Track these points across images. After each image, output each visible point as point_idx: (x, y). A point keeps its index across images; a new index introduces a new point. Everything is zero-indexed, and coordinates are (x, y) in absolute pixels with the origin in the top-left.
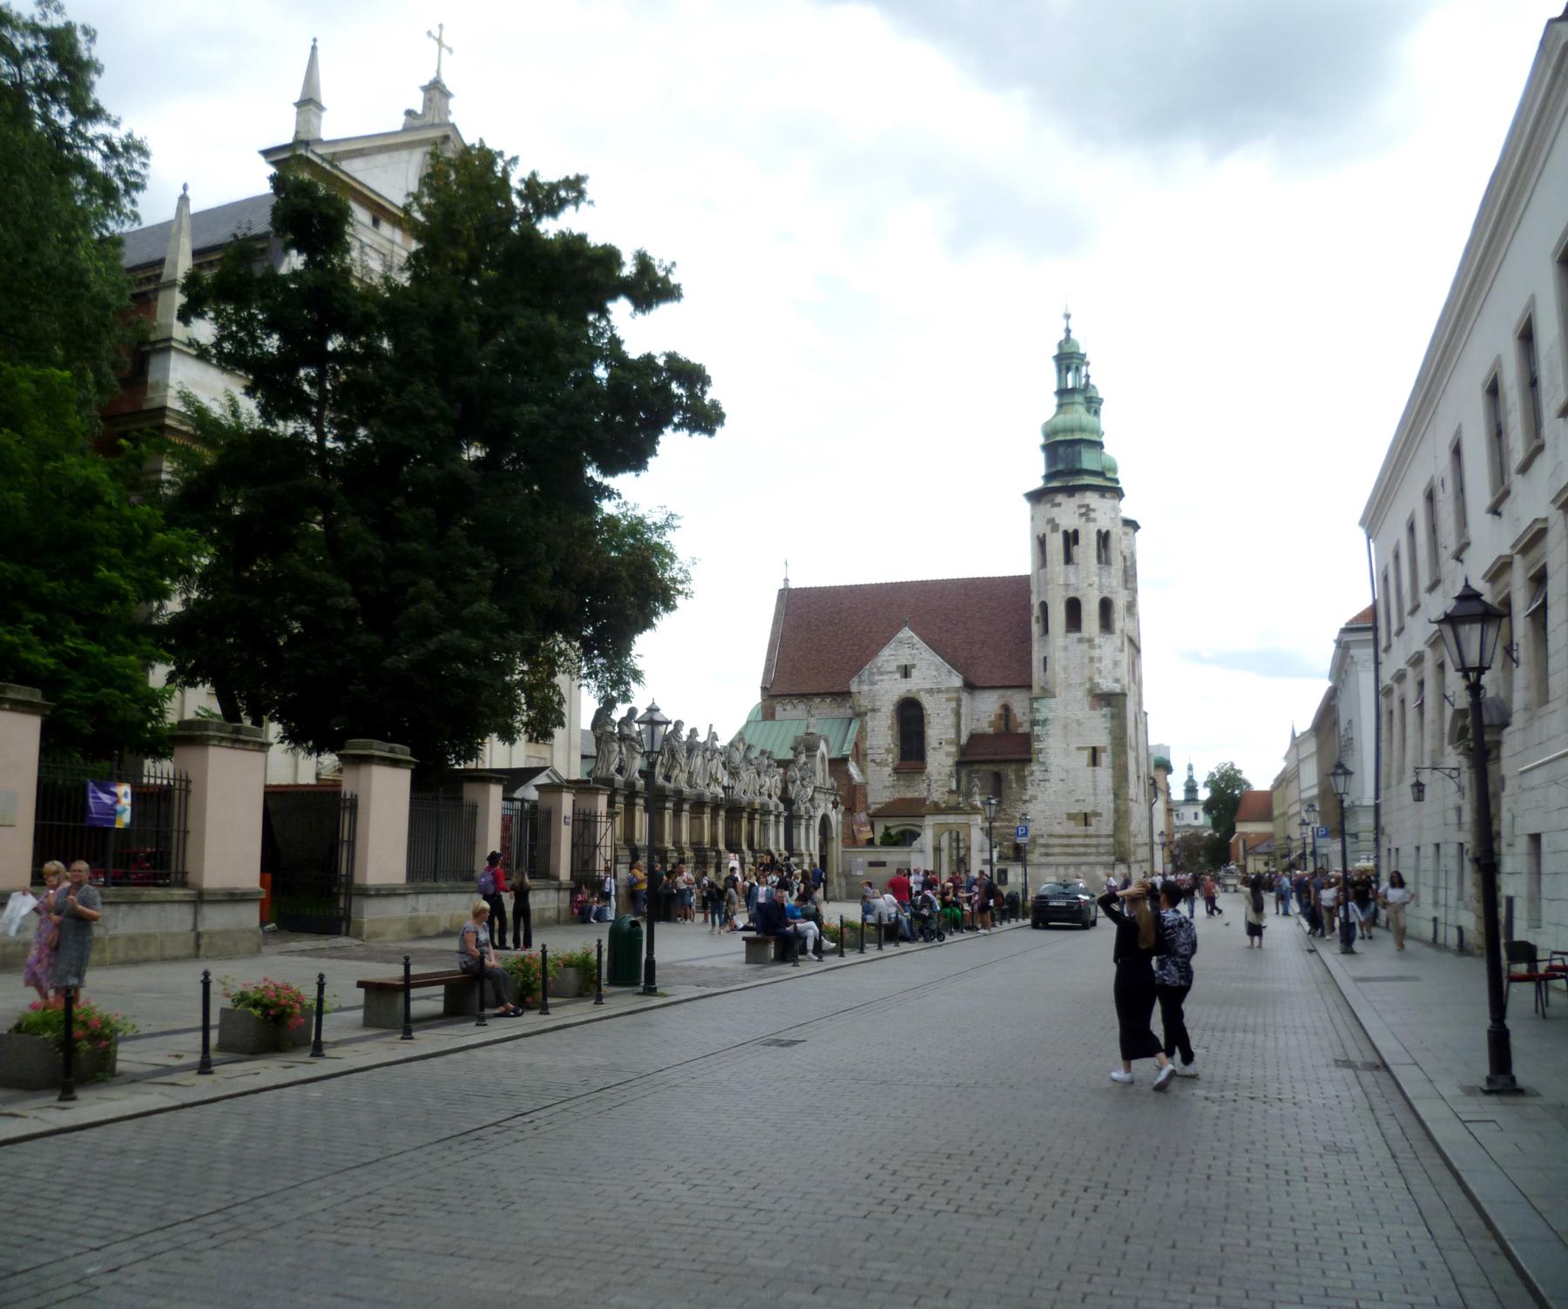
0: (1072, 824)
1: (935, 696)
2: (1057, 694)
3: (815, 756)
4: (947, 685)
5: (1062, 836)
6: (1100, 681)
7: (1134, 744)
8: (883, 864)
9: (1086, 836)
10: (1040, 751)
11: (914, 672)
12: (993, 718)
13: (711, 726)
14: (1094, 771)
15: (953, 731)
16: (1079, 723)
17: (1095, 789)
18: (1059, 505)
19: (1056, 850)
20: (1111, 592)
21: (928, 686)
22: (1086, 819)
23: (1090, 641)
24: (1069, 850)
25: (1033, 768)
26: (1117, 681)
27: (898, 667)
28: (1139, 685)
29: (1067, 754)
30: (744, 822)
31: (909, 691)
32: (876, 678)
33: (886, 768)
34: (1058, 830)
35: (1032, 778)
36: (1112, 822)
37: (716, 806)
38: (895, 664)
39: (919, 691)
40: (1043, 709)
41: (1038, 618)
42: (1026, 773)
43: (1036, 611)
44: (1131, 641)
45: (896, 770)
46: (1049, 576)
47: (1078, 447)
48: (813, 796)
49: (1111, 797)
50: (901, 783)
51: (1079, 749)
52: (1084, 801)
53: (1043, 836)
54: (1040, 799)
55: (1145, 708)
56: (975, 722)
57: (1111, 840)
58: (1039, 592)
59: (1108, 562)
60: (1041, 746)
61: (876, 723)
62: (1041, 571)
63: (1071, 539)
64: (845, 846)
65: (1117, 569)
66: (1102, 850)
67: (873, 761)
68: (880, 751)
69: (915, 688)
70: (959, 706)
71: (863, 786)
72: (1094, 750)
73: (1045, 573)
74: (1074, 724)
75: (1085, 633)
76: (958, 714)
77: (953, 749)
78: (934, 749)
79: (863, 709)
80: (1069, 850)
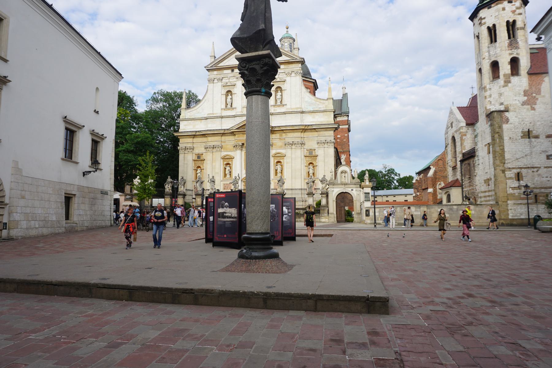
0: (485, 185)
6: (490, 107)
9: (489, 191)
11: (453, 125)
14: (489, 156)
19: (483, 199)
20: (496, 57)
22: (487, 181)
24: (485, 199)
26: (502, 104)
35: (477, 164)
40: (477, 129)
49: (493, 169)
51: (485, 145)
57: (493, 193)
59: (496, 41)
72: (489, 143)
75: (483, 86)
80: (485, 199)
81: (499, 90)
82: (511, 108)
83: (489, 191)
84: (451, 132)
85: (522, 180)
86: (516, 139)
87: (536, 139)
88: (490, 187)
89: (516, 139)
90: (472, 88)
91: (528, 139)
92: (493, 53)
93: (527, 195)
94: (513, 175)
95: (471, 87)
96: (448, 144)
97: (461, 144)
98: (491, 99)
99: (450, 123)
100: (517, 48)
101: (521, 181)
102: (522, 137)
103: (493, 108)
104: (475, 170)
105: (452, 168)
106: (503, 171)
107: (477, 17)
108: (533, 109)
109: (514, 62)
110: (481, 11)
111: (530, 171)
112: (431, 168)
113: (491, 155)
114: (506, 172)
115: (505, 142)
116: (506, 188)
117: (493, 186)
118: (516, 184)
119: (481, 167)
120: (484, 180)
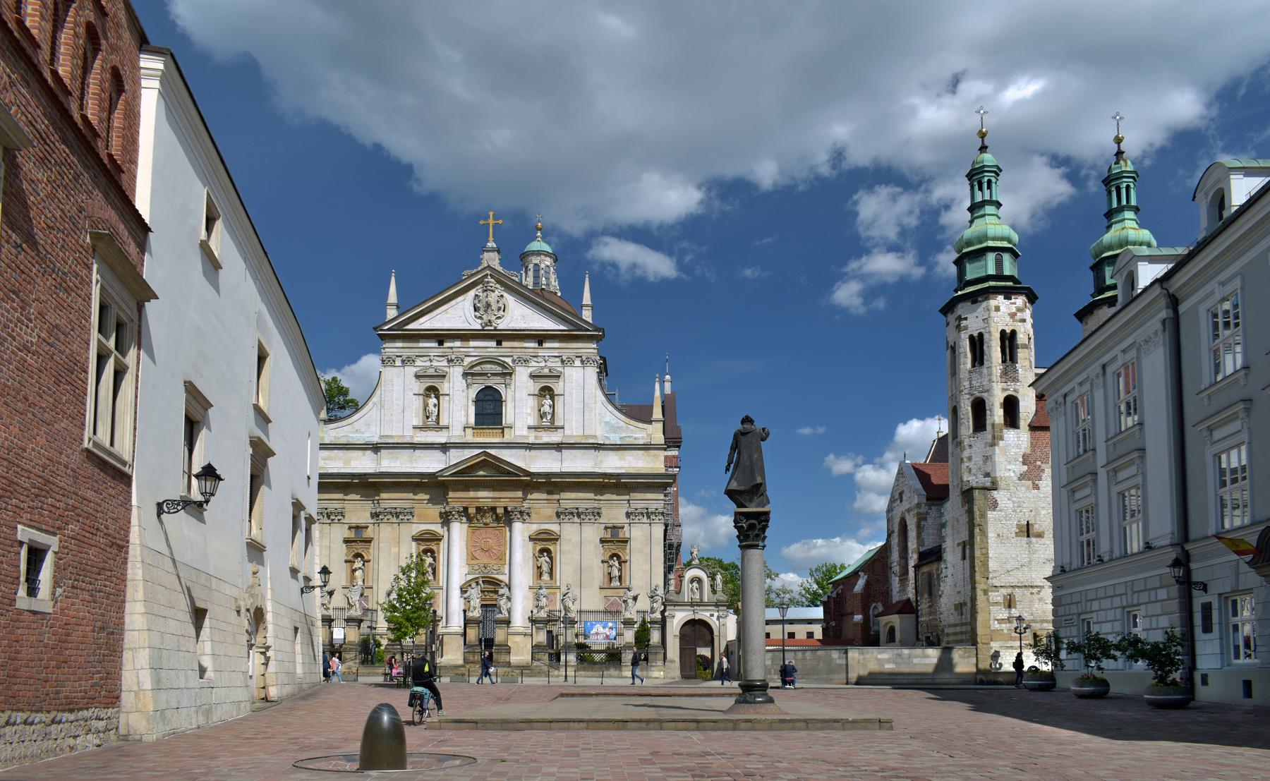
0: (956, 614)
9: (962, 624)
11: (904, 498)
15: (915, 541)
19: (951, 638)
21: (908, 506)
22: (960, 607)
26: (987, 475)
51: (958, 545)
57: (969, 628)
59: (982, 363)
72: (964, 542)
77: (915, 556)
82: (1001, 484)
83: (962, 624)
84: (900, 509)
85: (1015, 608)
86: (1008, 538)
87: (1038, 539)
88: (963, 617)
89: (1008, 538)
91: (1026, 539)
93: (1020, 634)
94: (1000, 599)
96: (893, 532)
97: (919, 535)
98: (971, 465)
99: (898, 492)
100: (1016, 380)
101: (1013, 610)
102: (1017, 534)
106: (986, 592)
107: (953, 312)
108: (1036, 487)
109: (1011, 405)
111: (1027, 592)
112: (859, 576)
113: (967, 562)
114: (990, 594)
115: (989, 541)
116: (989, 620)
117: (969, 616)
118: (1004, 614)
119: (949, 581)
120: (955, 605)
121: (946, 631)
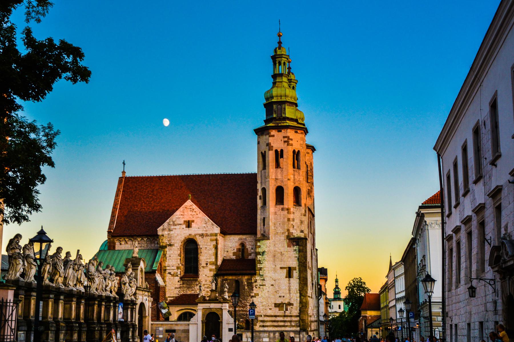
0: (277, 309)
1: (205, 238)
2: (270, 239)
3: (138, 269)
4: (211, 232)
5: (272, 316)
6: (293, 231)
7: (310, 266)
8: (174, 331)
9: (285, 316)
10: (261, 269)
11: (193, 225)
12: (235, 251)
13: (78, 251)
15: (214, 257)
16: (282, 254)
17: (290, 290)
18: (273, 136)
20: (299, 184)
21: (200, 232)
23: (288, 209)
24: (275, 324)
25: (257, 278)
26: (302, 231)
27: (185, 221)
28: (314, 234)
29: (275, 270)
30: (96, 307)
31: (190, 235)
32: (172, 227)
33: (177, 278)
34: (270, 312)
35: (256, 284)
36: (299, 308)
37: (79, 296)
38: (184, 220)
39: (195, 235)
41: (260, 196)
42: (253, 281)
43: (260, 193)
44: (310, 210)
45: (181, 278)
46: (267, 175)
47: (283, 105)
48: (136, 292)
49: (298, 295)
50: (185, 286)
51: (281, 268)
52: (284, 297)
53: (261, 316)
54: (260, 295)
55: (316, 247)
56: (226, 253)
58: (261, 183)
59: (299, 168)
60: (261, 266)
61: (172, 252)
62: (263, 171)
63: (279, 154)
64: (152, 320)
65: (302, 172)
66: (293, 324)
67: (170, 273)
68: (173, 268)
69: (193, 233)
70: (217, 243)
71: (164, 288)
72: (290, 268)
73: (265, 173)
74: (279, 255)
75: (286, 206)
76: (216, 248)
77: (214, 267)
78: (203, 267)
79: (164, 244)
80: (275, 324)
81: (300, 217)
90: (124, 164)
92: (298, 179)
95: (123, 162)
98: (294, 223)
103: (295, 233)
104: (253, 290)
105: (181, 278)
110: (289, 130)
112: (156, 273)
117: (298, 311)
119: (268, 288)
120: (275, 304)
121: (260, 319)
